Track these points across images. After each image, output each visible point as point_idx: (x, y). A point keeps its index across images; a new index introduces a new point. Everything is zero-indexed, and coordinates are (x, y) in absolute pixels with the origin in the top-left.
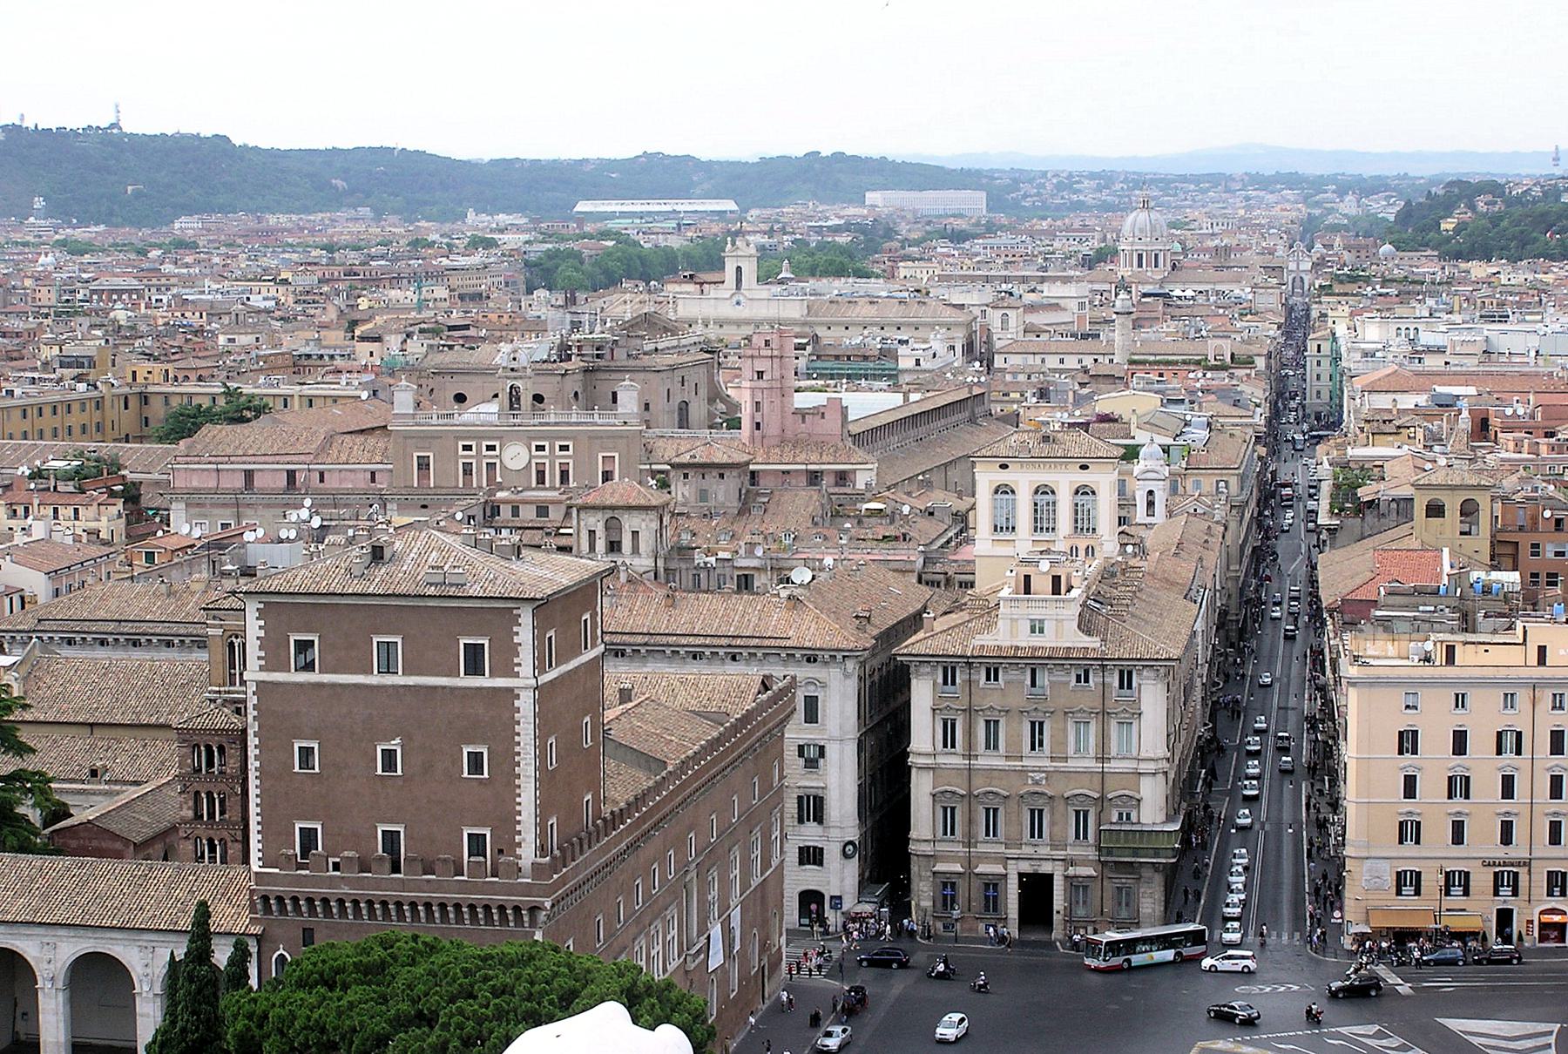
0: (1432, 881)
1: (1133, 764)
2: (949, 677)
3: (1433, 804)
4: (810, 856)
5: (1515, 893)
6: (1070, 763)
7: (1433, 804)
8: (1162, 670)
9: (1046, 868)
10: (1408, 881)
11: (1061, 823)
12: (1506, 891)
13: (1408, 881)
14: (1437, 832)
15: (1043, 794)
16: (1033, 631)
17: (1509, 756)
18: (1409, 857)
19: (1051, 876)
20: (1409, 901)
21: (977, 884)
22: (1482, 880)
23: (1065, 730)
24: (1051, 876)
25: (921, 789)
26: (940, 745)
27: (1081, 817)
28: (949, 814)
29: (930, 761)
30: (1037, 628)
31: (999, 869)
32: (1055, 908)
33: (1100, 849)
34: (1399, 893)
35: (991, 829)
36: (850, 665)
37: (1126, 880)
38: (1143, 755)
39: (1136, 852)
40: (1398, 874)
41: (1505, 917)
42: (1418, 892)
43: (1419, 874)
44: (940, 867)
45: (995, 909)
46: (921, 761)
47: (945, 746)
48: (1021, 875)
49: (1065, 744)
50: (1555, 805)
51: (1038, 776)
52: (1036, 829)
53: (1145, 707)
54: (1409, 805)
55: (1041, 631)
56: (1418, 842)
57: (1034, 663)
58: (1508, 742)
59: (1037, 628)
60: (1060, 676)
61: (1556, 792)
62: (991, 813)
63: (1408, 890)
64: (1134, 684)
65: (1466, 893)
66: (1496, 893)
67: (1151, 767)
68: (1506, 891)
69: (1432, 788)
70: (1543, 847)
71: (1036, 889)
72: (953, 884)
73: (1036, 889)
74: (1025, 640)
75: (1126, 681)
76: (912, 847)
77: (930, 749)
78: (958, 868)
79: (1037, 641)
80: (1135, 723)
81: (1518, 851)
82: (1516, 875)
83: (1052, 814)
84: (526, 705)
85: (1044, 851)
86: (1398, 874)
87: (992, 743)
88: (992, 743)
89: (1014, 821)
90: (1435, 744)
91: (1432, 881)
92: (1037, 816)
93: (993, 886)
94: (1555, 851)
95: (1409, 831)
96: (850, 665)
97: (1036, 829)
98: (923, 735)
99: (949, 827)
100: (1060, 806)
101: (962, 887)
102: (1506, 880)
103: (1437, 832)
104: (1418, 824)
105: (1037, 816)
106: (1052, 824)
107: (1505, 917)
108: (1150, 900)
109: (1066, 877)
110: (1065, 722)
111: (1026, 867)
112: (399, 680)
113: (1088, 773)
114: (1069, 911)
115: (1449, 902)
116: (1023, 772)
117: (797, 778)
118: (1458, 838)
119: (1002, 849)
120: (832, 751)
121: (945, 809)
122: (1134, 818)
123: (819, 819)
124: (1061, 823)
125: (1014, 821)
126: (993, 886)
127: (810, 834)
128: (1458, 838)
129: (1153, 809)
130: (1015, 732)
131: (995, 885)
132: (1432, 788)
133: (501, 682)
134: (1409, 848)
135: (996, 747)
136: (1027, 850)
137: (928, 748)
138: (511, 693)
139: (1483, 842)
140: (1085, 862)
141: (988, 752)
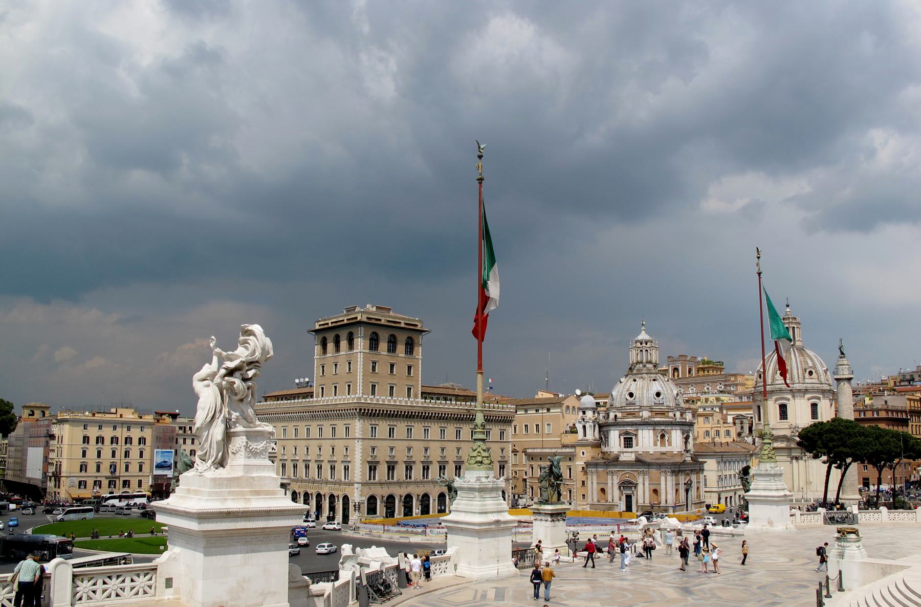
0: (90, 482)
10: (82, 484)
14: (92, 468)
17: (114, 445)
22: (105, 483)
58: (114, 440)
63: (82, 487)
70: (123, 473)
81: (117, 474)
91: (90, 482)
94: (127, 474)
95: (83, 467)
102: (112, 483)
103: (92, 468)
118: (98, 470)
128: (98, 470)
134: (83, 474)
139: (105, 471)
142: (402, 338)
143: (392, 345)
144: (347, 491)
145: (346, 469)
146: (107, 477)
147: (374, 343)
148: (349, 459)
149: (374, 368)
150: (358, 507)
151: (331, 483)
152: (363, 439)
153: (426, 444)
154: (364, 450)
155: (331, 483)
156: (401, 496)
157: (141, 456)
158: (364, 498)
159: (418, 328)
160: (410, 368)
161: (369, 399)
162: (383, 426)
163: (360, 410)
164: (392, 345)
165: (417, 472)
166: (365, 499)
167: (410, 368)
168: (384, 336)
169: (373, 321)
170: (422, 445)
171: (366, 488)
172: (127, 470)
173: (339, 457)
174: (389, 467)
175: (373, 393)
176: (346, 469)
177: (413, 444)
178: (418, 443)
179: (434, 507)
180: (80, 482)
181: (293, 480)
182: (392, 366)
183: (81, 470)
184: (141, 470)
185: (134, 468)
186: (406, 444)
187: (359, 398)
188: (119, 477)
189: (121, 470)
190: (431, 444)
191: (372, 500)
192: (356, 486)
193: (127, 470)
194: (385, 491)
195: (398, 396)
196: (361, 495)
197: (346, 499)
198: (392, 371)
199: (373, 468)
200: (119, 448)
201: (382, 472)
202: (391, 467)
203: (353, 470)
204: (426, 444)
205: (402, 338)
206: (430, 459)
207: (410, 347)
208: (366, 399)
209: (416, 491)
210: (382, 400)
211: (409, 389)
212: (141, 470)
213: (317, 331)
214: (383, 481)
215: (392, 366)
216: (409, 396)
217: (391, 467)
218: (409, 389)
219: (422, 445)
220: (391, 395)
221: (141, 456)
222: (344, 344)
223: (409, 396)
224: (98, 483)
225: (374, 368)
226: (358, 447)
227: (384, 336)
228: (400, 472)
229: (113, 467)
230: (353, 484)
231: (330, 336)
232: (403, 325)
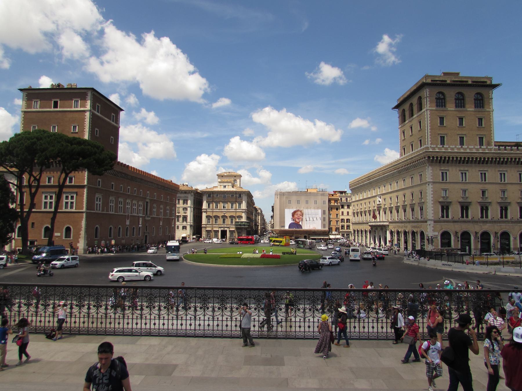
2: (209, 196)
4: (184, 228)
9: (226, 229)
11: (228, 221)
21: (213, 233)
24: (226, 231)
25: (204, 215)
30: (225, 187)
36: (192, 194)
37: (240, 231)
52: (224, 222)
60: (228, 195)
62: (216, 220)
74: (222, 189)
75: (240, 196)
84: (88, 114)
89: (220, 221)
92: (224, 220)
96: (192, 194)
97: (224, 222)
98: (205, 205)
100: (228, 218)
105: (224, 220)
109: (230, 231)
111: (222, 229)
112: (58, 109)
114: (231, 236)
116: (222, 212)
117: (182, 213)
120: (189, 209)
123: (186, 221)
124: (228, 221)
125: (220, 221)
127: (185, 223)
133: (82, 109)
137: (205, 208)
138: (84, 111)
140: (233, 228)
142: (470, 95)
143: (460, 102)
144: (422, 227)
145: (421, 209)
147: (441, 102)
148: (423, 201)
149: (442, 122)
150: (431, 241)
151: (413, 222)
152: (434, 182)
153: (503, 187)
154: (434, 192)
155: (413, 222)
156: (476, 233)
158: (436, 233)
159: (488, 83)
160: (480, 120)
161: (438, 149)
162: (454, 173)
163: (429, 157)
164: (460, 102)
165: (494, 212)
166: (438, 234)
167: (480, 120)
168: (450, 94)
169: (438, 82)
170: (498, 188)
171: (438, 225)
173: (416, 201)
174: (462, 208)
175: (442, 143)
176: (421, 209)
177: (487, 187)
178: (494, 186)
179: (515, 244)
181: (390, 222)
182: (461, 119)
186: (481, 187)
187: (427, 148)
190: (509, 187)
191: (445, 236)
192: (429, 223)
194: (460, 228)
195: (468, 145)
196: (434, 231)
197: (422, 234)
198: (461, 123)
199: (445, 207)
201: (455, 211)
202: (465, 208)
203: (426, 209)
204: (503, 187)
205: (470, 95)
206: (508, 201)
207: (481, 102)
208: (434, 148)
209: (494, 229)
210: (452, 148)
211: (481, 139)
213: (397, 107)
214: (456, 219)
215: (461, 119)
216: (481, 144)
217: (465, 208)
218: (481, 139)
219: (498, 188)
220: (462, 143)
222: (415, 108)
223: (481, 144)
225: (442, 122)
226: (429, 190)
227: (450, 94)
228: (475, 212)
230: (426, 222)
231: (406, 107)
232: (470, 82)
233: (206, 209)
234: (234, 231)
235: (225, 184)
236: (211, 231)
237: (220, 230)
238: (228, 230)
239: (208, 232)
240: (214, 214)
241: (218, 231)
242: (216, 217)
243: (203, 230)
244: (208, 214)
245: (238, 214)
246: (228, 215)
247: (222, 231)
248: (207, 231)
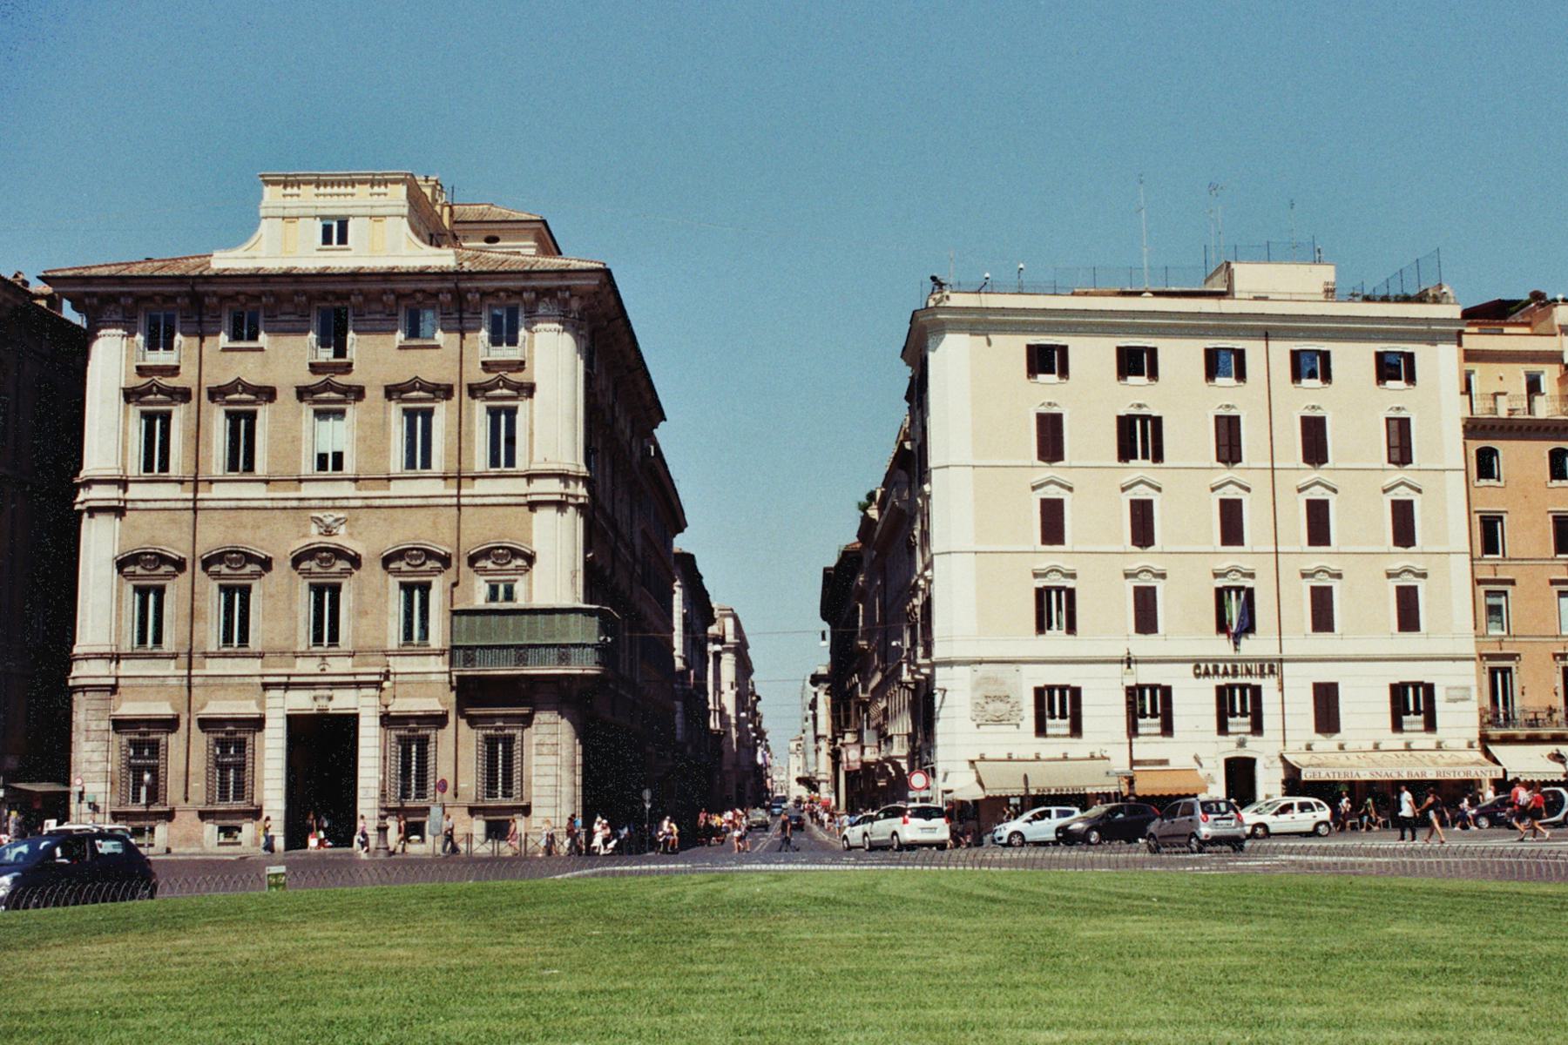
1: (520, 486)
3: (1098, 559)
5: (1257, 728)
6: (396, 488)
7: (1098, 559)
8: (575, 304)
9: (342, 702)
11: (373, 608)
12: (1239, 724)
13: (1058, 706)
15: (339, 553)
16: (327, 239)
18: (1052, 657)
19: (349, 723)
20: (1058, 743)
21: (201, 740)
22: (1194, 701)
23: (385, 425)
24: (349, 723)
26: (135, 468)
27: (416, 591)
28: (150, 597)
29: (110, 493)
30: (336, 231)
31: (248, 708)
32: (361, 783)
33: (454, 652)
34: (1041, 730)
35: (236, 630)
38: (538, 467)
39: (521, 652)
40: (1039, 692)
41: (1240, 775)
42: (1076, 730)
43: (1076, 693)
44: (129, 708)
45: (239, 795)
46: (98, 494)
47: (148, 467)
48: (297, 725)
49: (384, 453)
50: (1317, 558)
51: (329, 518)
52: (325, 628)
53: (538, 373)
54: (1052, 557)
55: (343, 239)
56: (1071, 628)
57: (333, 305)
59: (336, 231)
61: (1319, 531)
63: (1057, 726)
64: (522, 333)
65: (1167, 729)
66: (1223, 728)
67: (554, 487)
68: (1239, 724)
69: (1098, 518)
70: (1301, 638)
71: (322, 748)
72: (155, 747)
73: (322, 748)
76: (82, 672)
77: (114, 472)
78: (164, 709)
79: (340, 260)
80: (523, 406)
82: (1257, 691)
83: (359, 594)
85: (339, 666)
86: (1039, 692)
87: (241, 456)
88: (241, 456)
89: (281, 608)
90: (1092, 438)
92: (326, 597)
93: (232, 739)
94: (1323, 643)
95: (1054, 607)
97: (325, 628)
99: (149, 629)
100: (372, 572)
101: (174, 743)
102: (1238, 703)
104: (1071, 593)
105: (326, 597)
106: (361, 613)
107: (1240, 775)
108: (550, 757)
109: (387, 720)
110: (386, 411)
111: (302, 702)
113: (425, 505)
115: (1143, 749)
116: (301, 507)
118: (1146, 619)
119: (254, 666)
121: (143, 592)
122: (519, 588)
125: (281, 608)
126: (232, 739)
128: (1146, 619)
129: (556, 572)
130: (290, 434)
131: (241, 746)
132: (1098, 518)
134: (1056, 641)
135: (250, 466)
136: (307, 666)
139: (1188, 628)
140: (421, 683)
141: (234, 475)
146: (1203, 667)
157: (1404, 532)
172: (1323, 619)
180: (1043, 695)
183: (1043, 624)
184: (1408, 619)
185: (1365, 606)
188: (1271, 667)
189: (1282, 627)
193: (1323, 619)
200: (1259, 482)
212: (1408, 619)
221: (1404, 532)
224: (1149, 705)
229: (1235, 611)
233: (123, 483)
234: (439, 720)
235: (334, 202)
236: (171, 724)
237: (278, 708)
238: (366, 707)
239: (143, 740)
240: (213, 537)
241: (258, 724)
242: (236, 571)
243: (87, 717)
244: (137, 543)
245: (479, 531)
246: (366, 539)
247: (297, 725)
248: (119, 725)
